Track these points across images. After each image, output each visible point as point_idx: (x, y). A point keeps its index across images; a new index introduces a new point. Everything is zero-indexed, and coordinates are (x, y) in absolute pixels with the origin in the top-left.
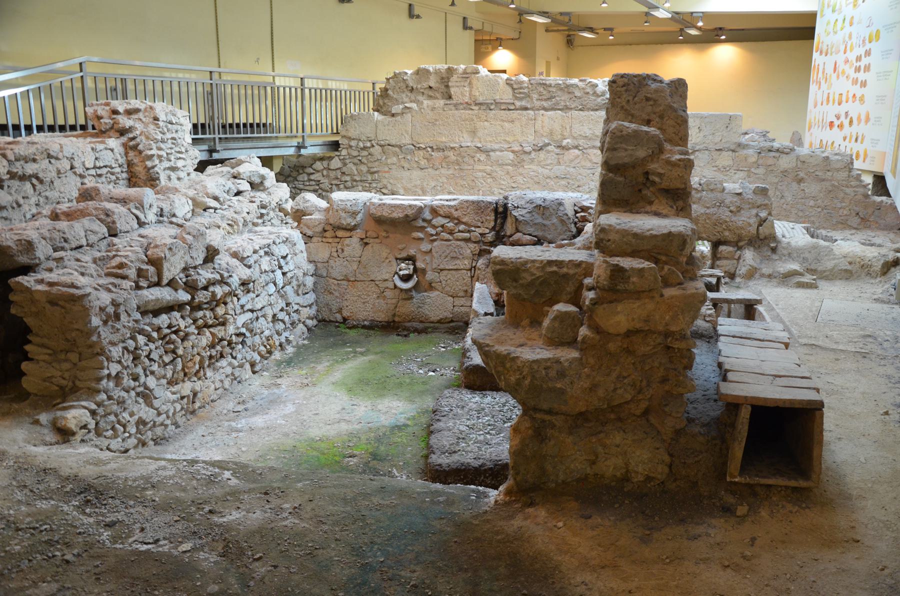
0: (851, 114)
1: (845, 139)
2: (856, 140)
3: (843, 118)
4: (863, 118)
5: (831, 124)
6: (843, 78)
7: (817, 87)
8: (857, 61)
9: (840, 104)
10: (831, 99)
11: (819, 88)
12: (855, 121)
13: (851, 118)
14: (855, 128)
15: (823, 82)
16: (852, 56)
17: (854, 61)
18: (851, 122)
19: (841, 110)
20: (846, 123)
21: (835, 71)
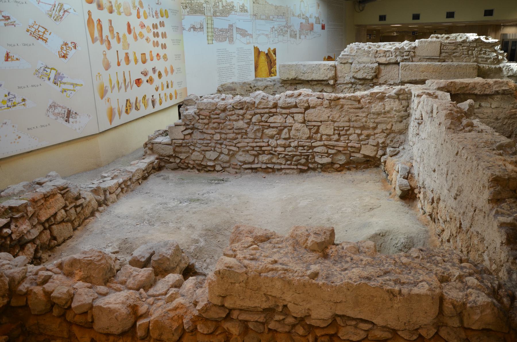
0: (158, 69)
1: (157, 89)
2: (168, 87)
3: (151, 73)
4: (169, 70)
5: (138, 82)
6: (141, 41)
7: (104, 47)
8: (153, 28)
9: (144, 62)
10: (131, 57)
11: (109, 47)
12: (163, 73)
13: (160, 72)
14: (164, 79)
15: (114, 42)
16: (149, 22)
17: (151, 27)
18: (160, 75)
19: (149, 66)
20: (155, 76)
21: (130, 31)
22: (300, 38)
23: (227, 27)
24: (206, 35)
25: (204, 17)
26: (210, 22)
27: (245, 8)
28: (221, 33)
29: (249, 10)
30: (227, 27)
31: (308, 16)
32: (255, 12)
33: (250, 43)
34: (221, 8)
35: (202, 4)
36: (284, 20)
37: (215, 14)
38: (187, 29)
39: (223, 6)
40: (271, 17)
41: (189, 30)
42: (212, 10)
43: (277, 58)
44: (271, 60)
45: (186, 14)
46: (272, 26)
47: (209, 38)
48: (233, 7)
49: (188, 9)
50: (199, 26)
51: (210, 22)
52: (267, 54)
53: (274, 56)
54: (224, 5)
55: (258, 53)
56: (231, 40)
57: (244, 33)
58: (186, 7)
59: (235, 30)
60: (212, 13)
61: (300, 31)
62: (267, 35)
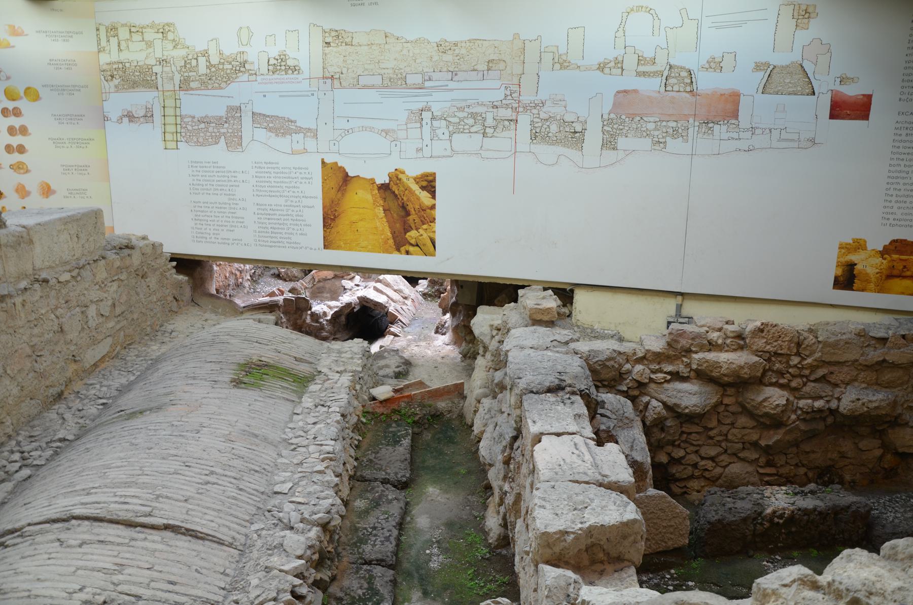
22: (609, 144)
23: (222, 112)
24: (159, 130)
25: (156, 94)
26: (170, 103)
27: (290, 63)
28: (202, 126)
29: (304, 66)
30: (222, 112)
31: (686, 59)
32: (332, 70)
33: (305, 151)
34: (203, 69)
35: (150, 68)
36: (497, 84)
37: (185, 85)
38: (114, 119)
39: (210, 66)
40: (411, 80)
41: (120, 120)
42: (177, 78)
43: (439, 201)
44: (403, 207)
45: (113, 90)
46: (420, 106)
47: (169, 137)
48: (244, 64)
49: (116, 81)
50: (142, 113)
51: (170, 103)
52: (384, 187)
53: (424, 197)
54: (215, 60)
55: (339, 181)
56: (235, 142)
57: (280, 126)
58: (112, 77)
59: (247, 120)
60: (177, 83)
61: (607, 122)
62: (387, 132)
